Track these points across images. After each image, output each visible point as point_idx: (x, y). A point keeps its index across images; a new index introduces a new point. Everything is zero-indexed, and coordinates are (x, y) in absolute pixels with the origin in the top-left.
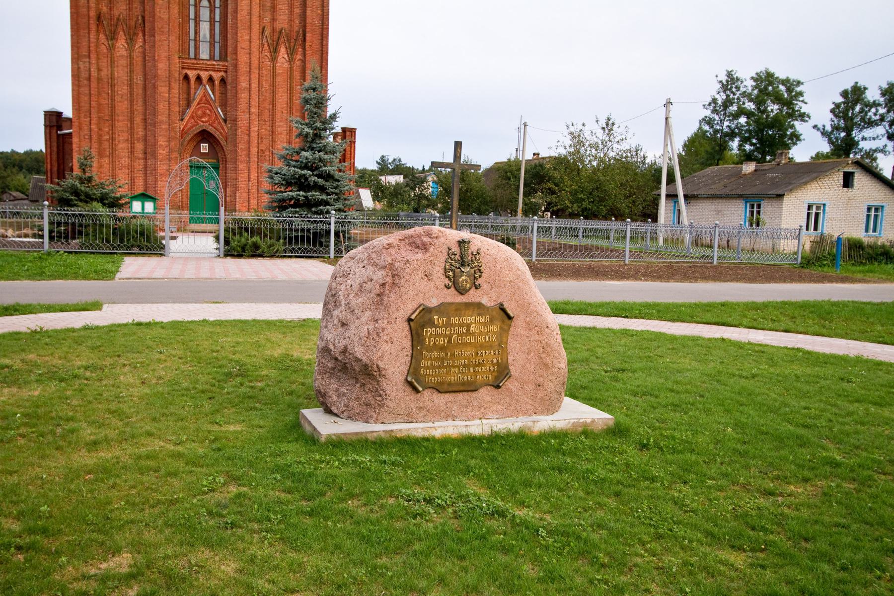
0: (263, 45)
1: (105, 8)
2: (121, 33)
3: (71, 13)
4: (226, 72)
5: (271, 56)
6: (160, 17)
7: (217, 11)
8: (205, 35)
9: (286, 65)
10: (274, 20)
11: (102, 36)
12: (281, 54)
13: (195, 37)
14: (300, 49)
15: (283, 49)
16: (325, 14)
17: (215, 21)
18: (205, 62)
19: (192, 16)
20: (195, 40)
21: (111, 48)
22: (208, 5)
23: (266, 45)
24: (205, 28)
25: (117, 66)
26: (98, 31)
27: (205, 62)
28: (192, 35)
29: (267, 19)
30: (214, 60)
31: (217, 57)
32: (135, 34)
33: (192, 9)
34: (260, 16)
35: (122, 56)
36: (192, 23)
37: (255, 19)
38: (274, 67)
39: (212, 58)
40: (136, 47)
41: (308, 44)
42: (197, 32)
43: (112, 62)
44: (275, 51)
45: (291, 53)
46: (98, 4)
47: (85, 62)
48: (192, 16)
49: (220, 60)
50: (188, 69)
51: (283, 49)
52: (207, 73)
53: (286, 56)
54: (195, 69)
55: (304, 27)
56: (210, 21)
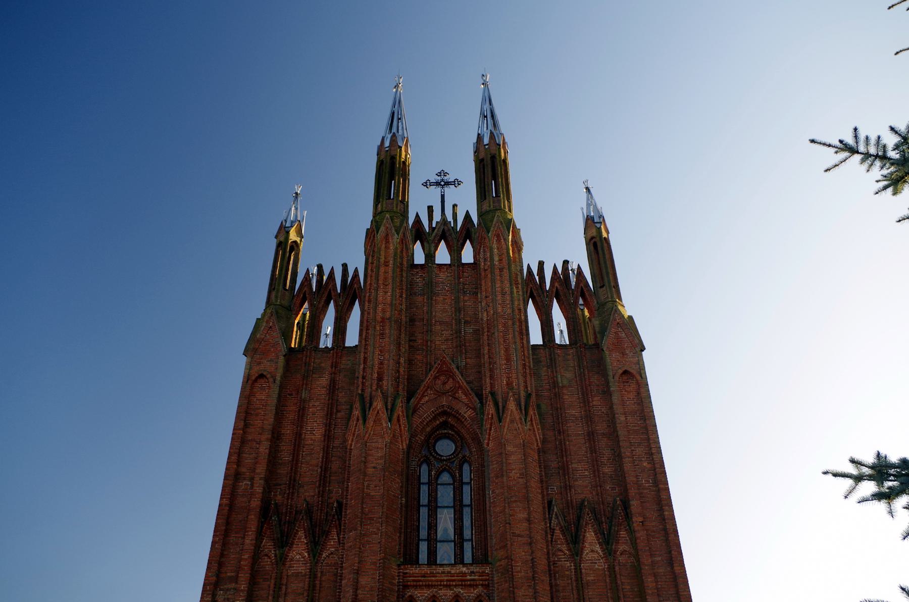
0: (553, 531)
1: (279, 497)
2: (301, 534)
3: (220, 505)
4: (486, 586)
5: (569, 550)
6: (368, 495)
7: (466, 489)
8: (446, 530)
9: (601, 565)
10: (567, 487)
11: (267, 544)
12: (587, 545)
13: (429, 534)
14: (623, 533)
15: (590, 536)
16: (657, 466)
17: (462, 506)
18: (447, 569)
19: (424, 500)
20: (429, 540)
21: (282, 560)
22: (452, 482)
23: (558, 532)
24: (446, 521)
25: (285, 594)
26: (260, 535)
27: (447, 569)
28: (423, 534)
29: (555, 487)
30: (464, 565)
31: (468, 557)
32: (327, 533)
33: (424, 489)
34: (542, 482)
35: (297, 575)
36: (424, 512)
37: (534, 484)
38: (578, 570)
39: (459, 559)
40: (324, 555)
41: (637, 519)
42: (432, 526)
43: (278, 587)
44: (575, 540)
45: (607, 541)
46: (270, 492)
47: (228, 590)
48: (424, 500)
49: (475, 561)
50: (416, 587)
51: (590, 536)
52: (450, 593)
53: (597, 548)
54: (429, 587)
55: (625, 491)
56: (454, 507)
